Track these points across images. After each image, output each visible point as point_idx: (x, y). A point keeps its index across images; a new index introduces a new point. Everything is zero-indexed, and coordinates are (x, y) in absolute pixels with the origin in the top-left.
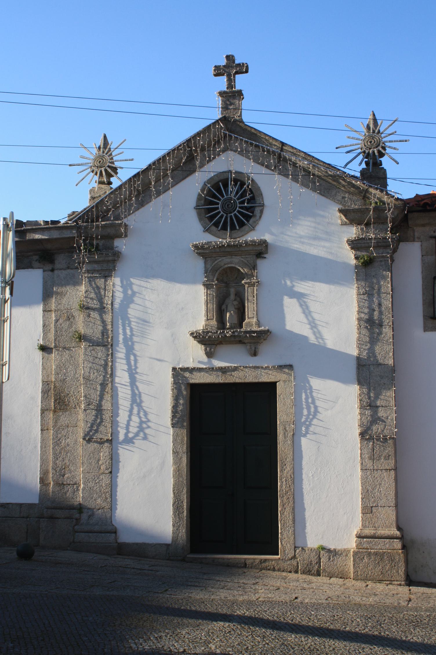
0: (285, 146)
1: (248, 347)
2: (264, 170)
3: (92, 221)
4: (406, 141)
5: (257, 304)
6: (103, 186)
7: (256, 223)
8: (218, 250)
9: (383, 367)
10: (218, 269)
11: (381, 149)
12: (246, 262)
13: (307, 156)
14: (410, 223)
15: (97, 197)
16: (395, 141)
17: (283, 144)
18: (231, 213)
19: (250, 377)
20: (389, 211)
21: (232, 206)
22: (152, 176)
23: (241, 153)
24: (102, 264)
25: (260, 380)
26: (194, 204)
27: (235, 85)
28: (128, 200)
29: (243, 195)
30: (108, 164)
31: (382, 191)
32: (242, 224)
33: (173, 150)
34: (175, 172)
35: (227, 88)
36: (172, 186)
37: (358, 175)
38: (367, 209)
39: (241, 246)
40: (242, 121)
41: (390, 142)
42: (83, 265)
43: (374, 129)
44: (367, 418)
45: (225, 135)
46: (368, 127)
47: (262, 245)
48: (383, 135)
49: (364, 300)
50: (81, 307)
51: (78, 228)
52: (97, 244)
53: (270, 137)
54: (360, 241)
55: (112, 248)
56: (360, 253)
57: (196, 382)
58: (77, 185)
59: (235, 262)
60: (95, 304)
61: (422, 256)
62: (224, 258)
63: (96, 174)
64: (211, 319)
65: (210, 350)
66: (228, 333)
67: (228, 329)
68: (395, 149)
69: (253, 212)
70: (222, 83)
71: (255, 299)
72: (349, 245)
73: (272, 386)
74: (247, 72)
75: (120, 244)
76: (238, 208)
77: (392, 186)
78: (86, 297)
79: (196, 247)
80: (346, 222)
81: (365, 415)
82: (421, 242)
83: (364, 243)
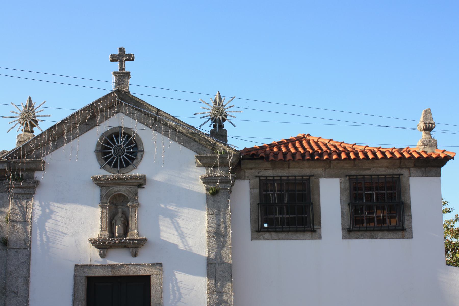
0: (159, 112)
1: (131, 250)
2: (144, 127)
3: (19, 158)
4: (240, 112)
5: (137, 220)
6: (27, 133)
7: (138, 163)
8: (111, 182)
9: (225, 264)
10: (110, 195)
11: (224, 117)
12: (131, 190)
13: (174, 119)
14: (242, 166)
15: (23, 141)
16: (235, 112)
17: (158, 110)
18: (121, 156)
19: (132, 272)
20: (230, 159)
21: (121, 151)
23: (129, 115)
24: (25, 190)
25: (139, 274)
26: (94, 149)
27: (125, 68)
28: (46, 144)
29: (130, 143)
31: (225, 145)
32: (128, 164)
33: (81, 111)
34: (82, 126)
35: (119, 70)
36: (79, 136)
37: (209, 133)
38: (215, 156)
39: (127, 179)
40: (129, 93)
41: (230, 112)
42: (11, 189)
43: (219, 103)
44: (214, 300)
45: (118, 102)
46: (215, 101)
47: (142, 179)
48: (225, 107)
49: (212, 218)
50: (7, 220)
51: (8, 163)
52: (22, 175)
53: (150, 105)
54: (210, 178)
55: (33, 178)
56: (209, 186)
57: (92, 276)
58: (8, 132)
59: (123, 190)
60: (19, 218)
61: (250, 189)
62: (115, 187)
63: (23, 125)
64: (104, 231)
65: (103, 252)
67: (117, 237)
68: (233, 117)
69: (136, 156)
70: (116, 66)
71: (136, 216)
72: (202, 180)
73: (148, 278)
74: (133, 60)
75: (38, 175)
76: (125, 153)
77: (230, 141)
78: (11, 213)
79: (95, 179)
80: (200, 165)
81: (212, 298)
82: (250, 179)
83: (213, 179)
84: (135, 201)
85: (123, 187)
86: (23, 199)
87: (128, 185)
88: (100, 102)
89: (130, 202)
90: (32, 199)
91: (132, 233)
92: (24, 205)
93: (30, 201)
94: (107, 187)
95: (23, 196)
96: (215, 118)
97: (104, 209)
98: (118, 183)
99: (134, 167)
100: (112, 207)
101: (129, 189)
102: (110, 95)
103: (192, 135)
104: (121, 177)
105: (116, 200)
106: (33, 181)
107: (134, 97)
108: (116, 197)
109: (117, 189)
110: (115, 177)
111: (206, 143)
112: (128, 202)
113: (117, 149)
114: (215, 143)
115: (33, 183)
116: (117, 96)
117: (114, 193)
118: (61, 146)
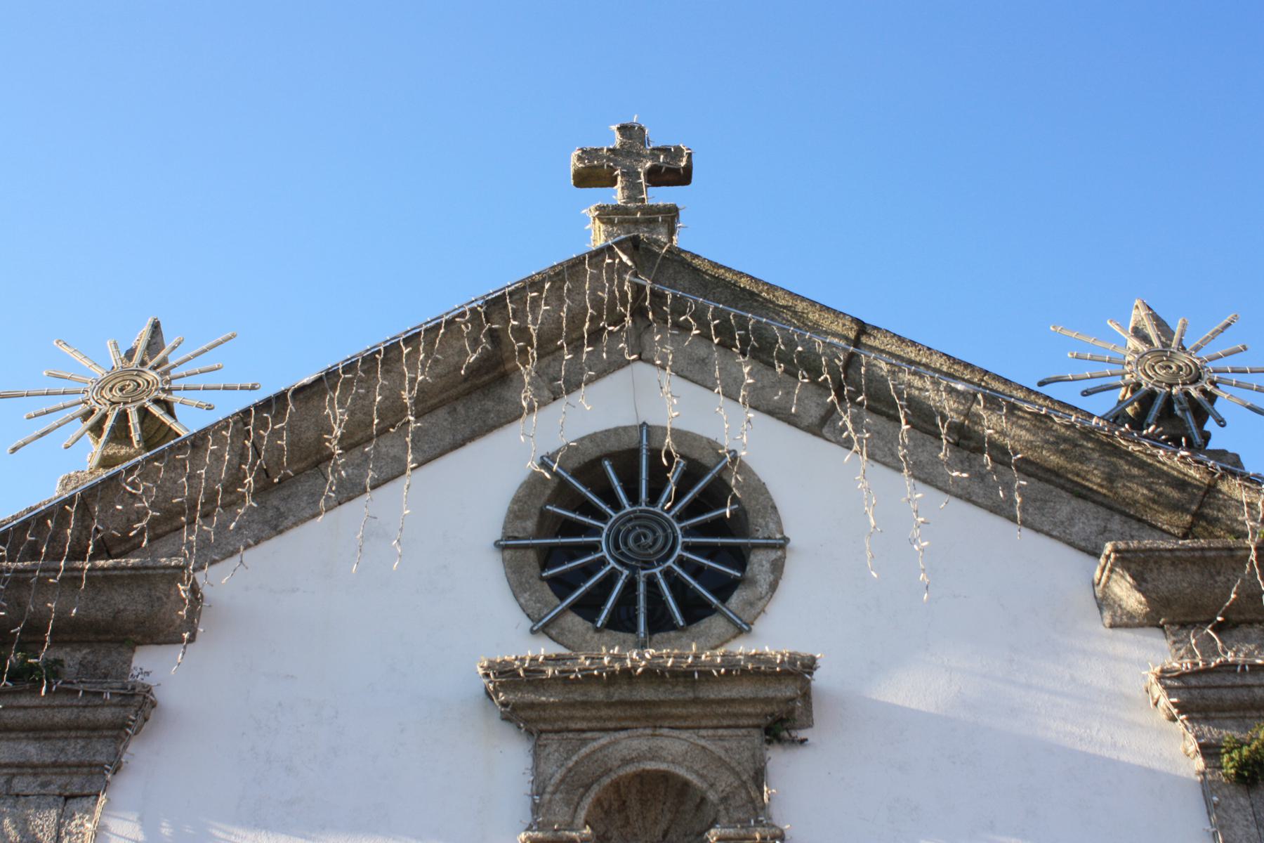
0: (870, 335)
10: (597, 779)
12: (722, 754)
17: (863, 328)
18: (648, 565)
21: (655, 542)
22: (337, 416)
24: (60, 744)
26: (495, 532)
30: (154, 395)
38: (1230, 549)
39: (705, 675)
45: (638, 290)
53: (813, 303)
54: (1215, 679)
56: (1215, 732)
58: (15, 450)
62: (623, 734)
72: (1169, 690)
76: (678, 551)
83: (1233, 687)
84: (757, 809)
85: (676, 733)
86: (42, 799)
87: (704, 723)
88: (540, 290)
89: (724, 821)
90: (97, 800)
92: (40, 835)
93: (86, 812)
94: (570, 735)
95: (43, 785)
96: (1162, 391)
98: (643, 704)
99: (735, 624)
102: (594, 260)
103: (1063, 452)
104: (669, 664)
105: (627, 822)
106: (119, 685)
107: (722, 271)
108: (624, 802)
109: (635, 743)
110: (632, 660)
111: (1152, 495)
112: (712, 826)
113: (629, 532)
114: (1211, 489)
115: (116, 700)
116: (630, 263)
117: (619, 767)
118: (304, 520)
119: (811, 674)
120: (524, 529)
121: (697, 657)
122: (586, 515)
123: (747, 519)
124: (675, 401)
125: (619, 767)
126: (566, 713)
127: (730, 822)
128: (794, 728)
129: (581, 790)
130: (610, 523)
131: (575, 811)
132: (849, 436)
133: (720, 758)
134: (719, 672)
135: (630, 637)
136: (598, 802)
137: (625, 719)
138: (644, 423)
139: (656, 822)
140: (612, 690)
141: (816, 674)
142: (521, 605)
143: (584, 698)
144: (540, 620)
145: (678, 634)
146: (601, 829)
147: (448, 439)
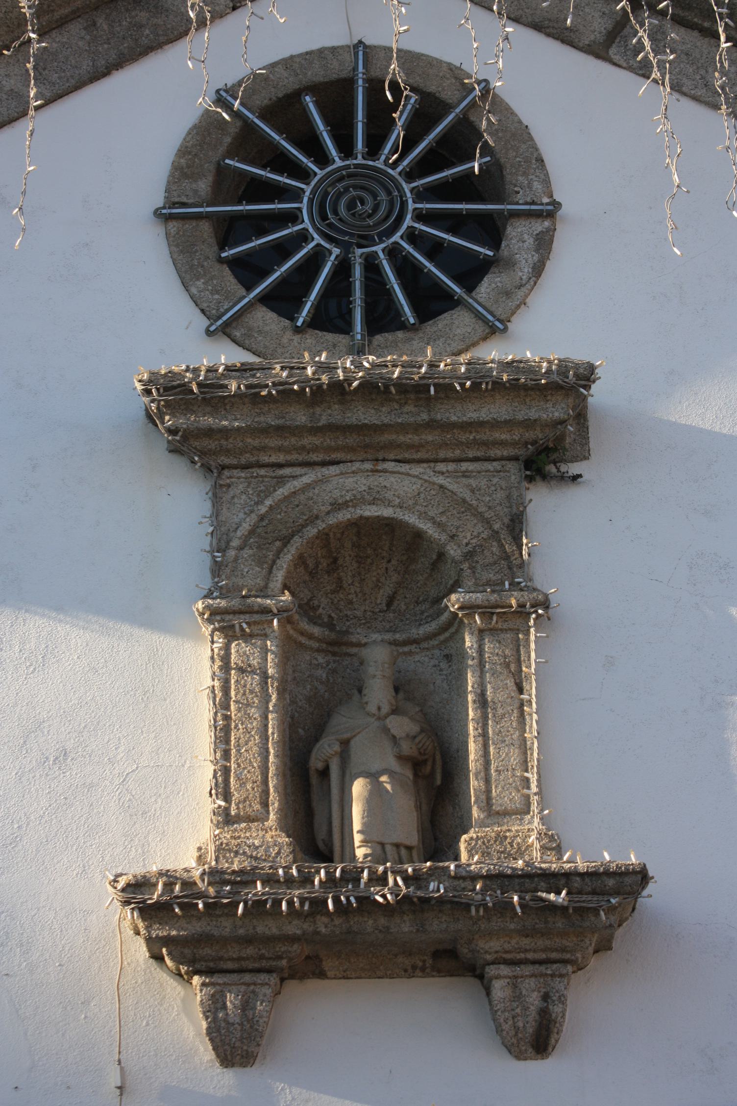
10: (299, 530)
12: (468, 496)
18: (366, 240)
21: (376, 208)
39: (445, 390)
62: (333, 470)
64: (250, 819)
65: (246, 1006)
66: (382, 880)
76: (408, 221)
85: (405, 468)
87: (442, 454)
89: (469, 582)
91: (500, 838)
94: (262, 472)
97: (247, 637)
100: (311, 637)
101: (453, 487)
105: (339, 587)
108: (335, 560)
109: (349, 482)
110: (345, 369)
112: (452, 590)
113: (339, 195)
117: (328, 513)
119: (587, 387)
120: (196, 192)
121: (432, 365)
122: (280, 172)
123: (502, 177)
124: (403, 10)
125: (328, 513)
126: (256, 443)
127: (476, 584)
128: (565, 461)
129: (278, 544)
130: (313, 183)
131: (270, 572)
132: (646, 57)
133: (464, 501)
134: (462, 385)
135: (342, 340)
136: (301, 560)
137: (337, 449)
138: (360, 42)
139: (377, 586)
140: (318, 410)
141: (594, 388)
142: (192, 297)
143: (280, 422)
144: (219, 318)
145: (408, 335)
146: (305, 594)
147: (86, 65)
